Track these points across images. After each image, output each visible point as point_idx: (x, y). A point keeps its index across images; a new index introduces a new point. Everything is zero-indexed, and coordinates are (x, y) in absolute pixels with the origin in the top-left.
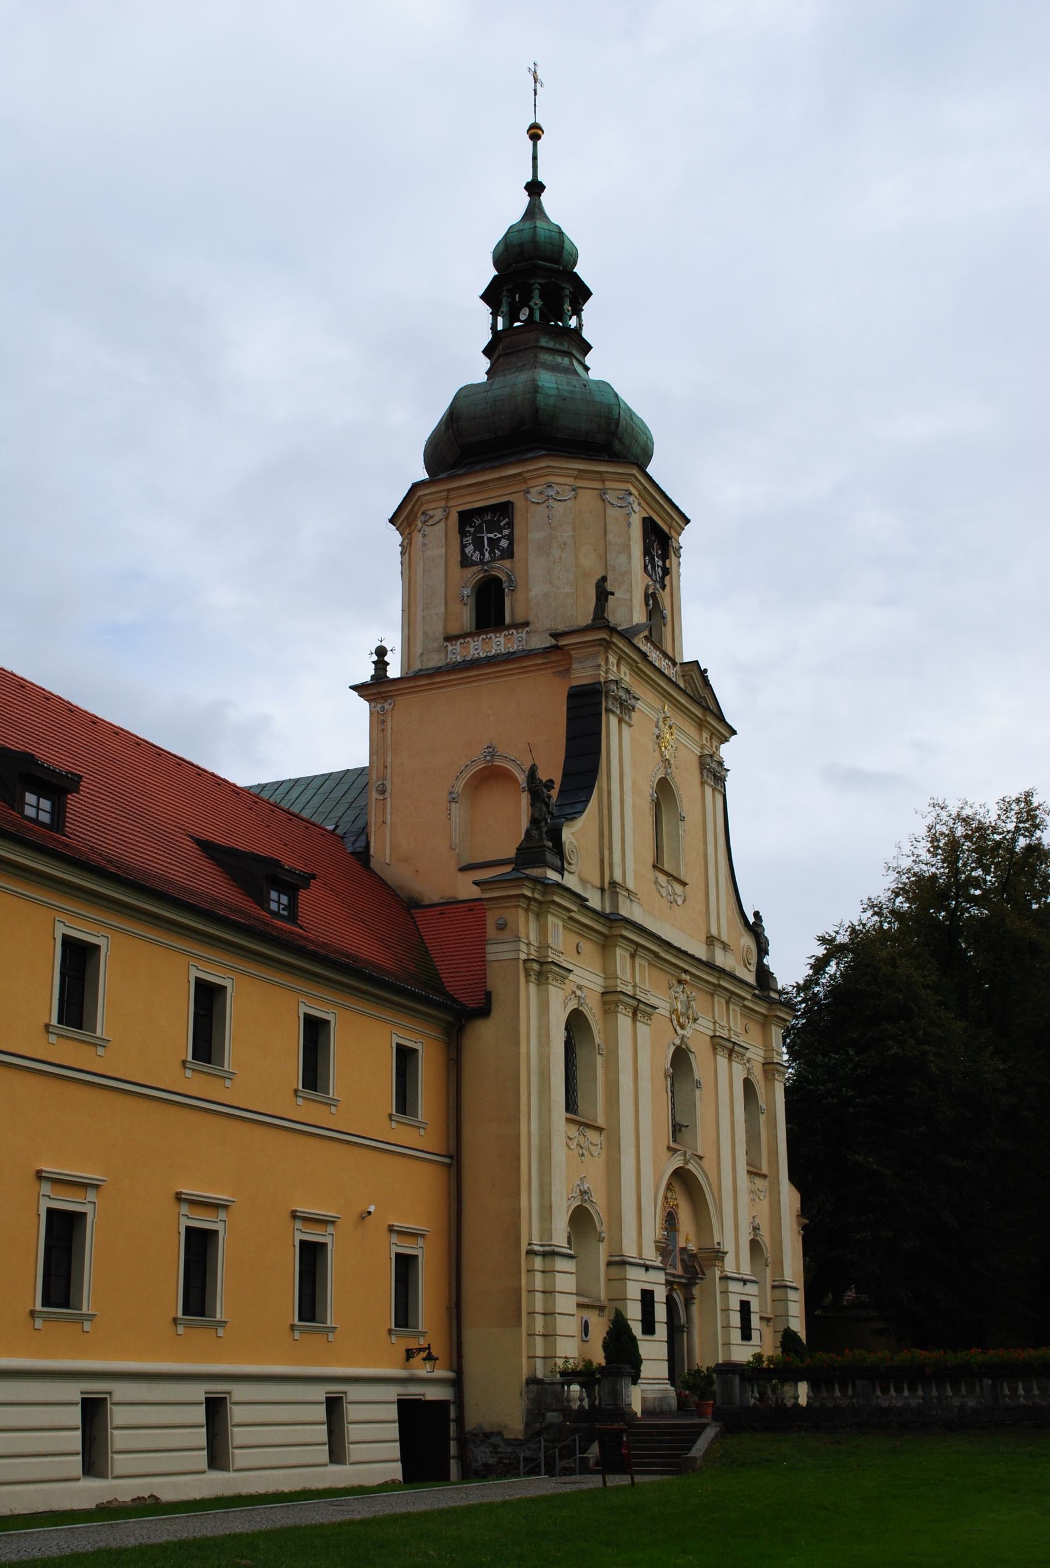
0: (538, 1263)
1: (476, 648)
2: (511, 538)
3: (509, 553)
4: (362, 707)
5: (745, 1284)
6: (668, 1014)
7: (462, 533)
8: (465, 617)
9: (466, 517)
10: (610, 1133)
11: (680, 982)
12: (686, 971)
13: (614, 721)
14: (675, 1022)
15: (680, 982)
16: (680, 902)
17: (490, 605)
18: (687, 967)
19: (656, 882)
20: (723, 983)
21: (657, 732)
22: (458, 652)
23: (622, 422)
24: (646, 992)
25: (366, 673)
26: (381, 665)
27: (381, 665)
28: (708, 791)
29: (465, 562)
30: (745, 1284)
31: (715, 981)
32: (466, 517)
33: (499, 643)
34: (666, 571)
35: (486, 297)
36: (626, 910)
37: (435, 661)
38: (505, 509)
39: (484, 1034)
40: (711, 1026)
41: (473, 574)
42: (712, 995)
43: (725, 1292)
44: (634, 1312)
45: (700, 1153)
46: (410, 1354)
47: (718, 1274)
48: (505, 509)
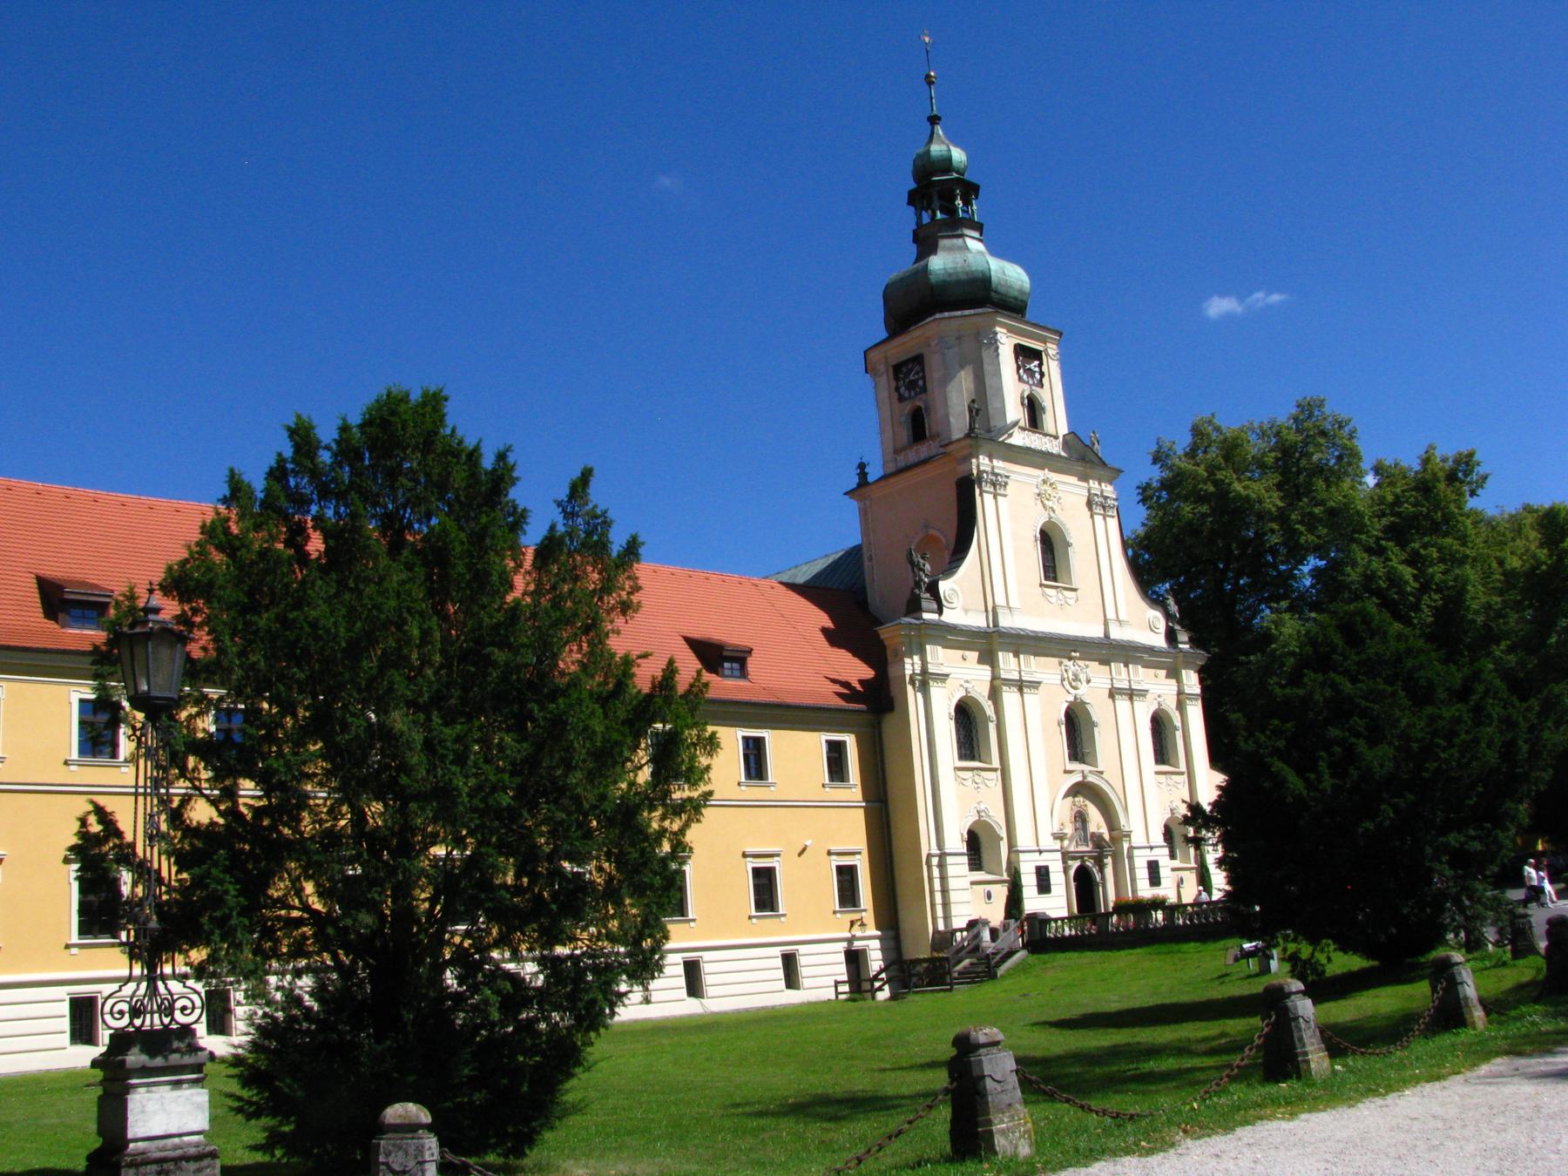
1: (911, 456)
2: (924, 378)
3: (924, 389)
4: (853, 506)
7: (897, 379)
8: (904, 435)
9: (898, 370)
13: (988, 498)
16: (1071, 602)
17: (919, 427)
19: (1044, 594)
22: (902, 461)
23: (994, 279)
24: (1031, 673)
25: (854, 481)
26: (863, 474)
27: (863, 474)
28: (1099, 519)
29: (901, 399)
32: (898, 370)
33: (924, 450)
34: (1042, 375)
35: (909, 203)
36: (1006, 622)
37: (891, 468)
38: (918, 360)
39: (889, 723)
41: (907, 407)
43: (1131, 857)
46: (852, 923)
47: (1126, 846)
48: (918, 360)
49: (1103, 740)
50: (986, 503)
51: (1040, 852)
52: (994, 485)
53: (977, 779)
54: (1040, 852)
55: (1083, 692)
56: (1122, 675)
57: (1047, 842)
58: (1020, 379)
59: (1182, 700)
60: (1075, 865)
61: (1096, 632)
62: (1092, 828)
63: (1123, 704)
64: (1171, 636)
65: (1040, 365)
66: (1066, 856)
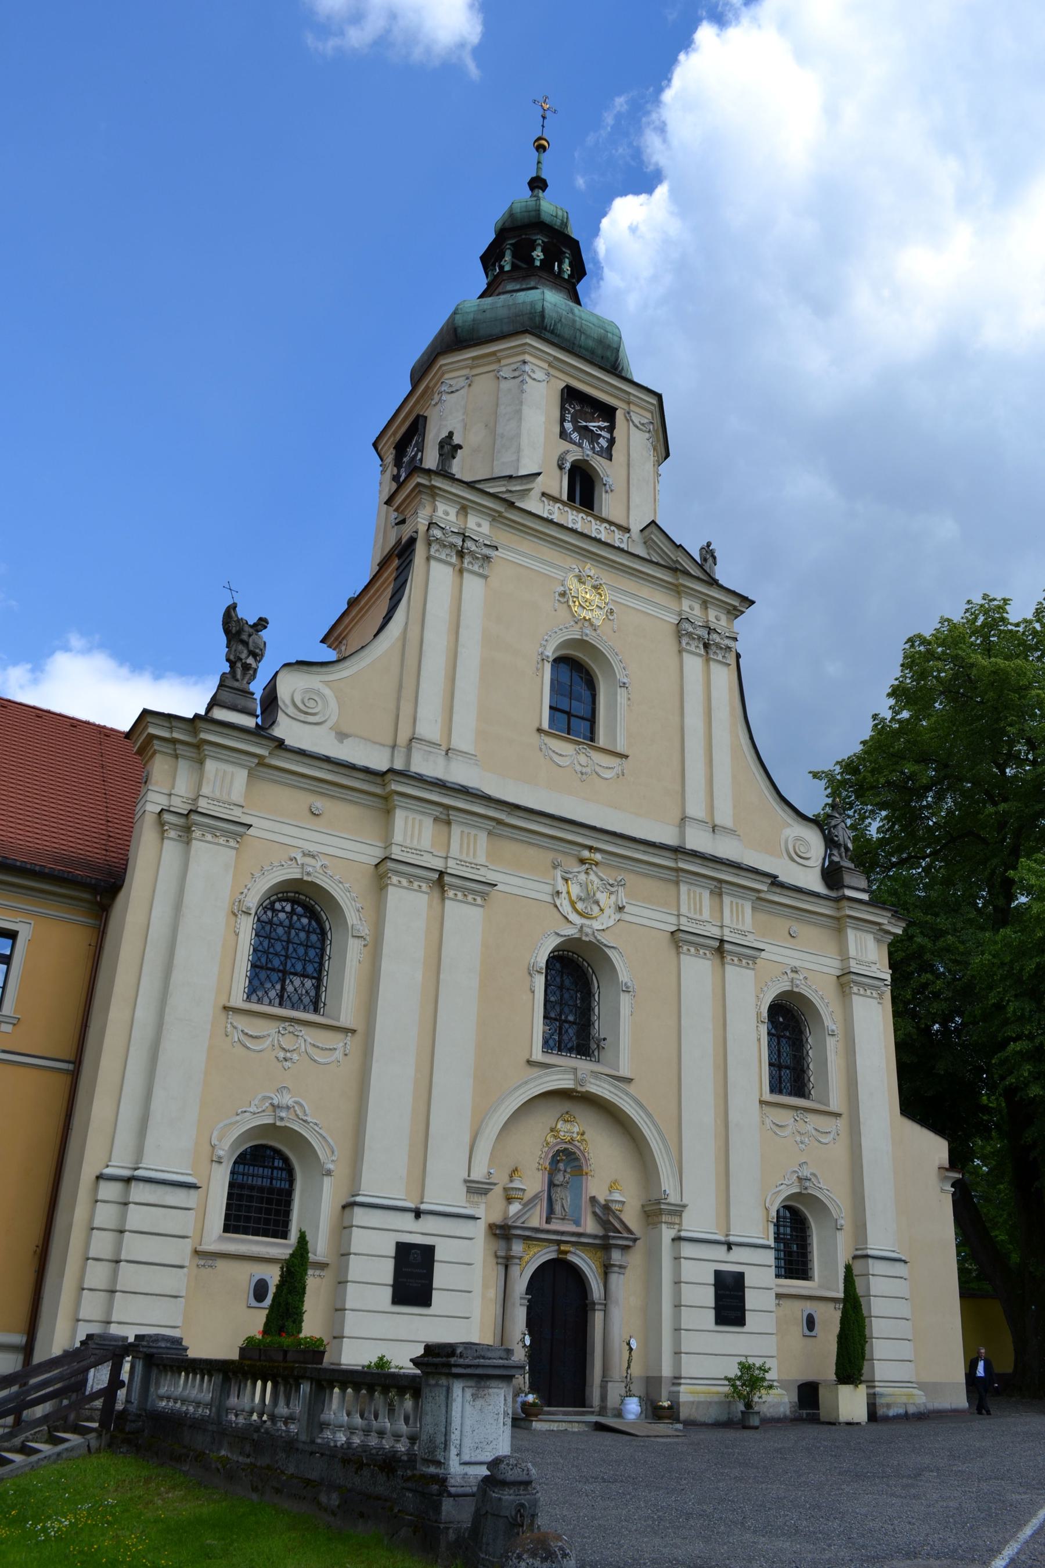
0: (109, 1191)
5: (729, 1248)
6: (549, 899)
10: (363, 1036)
11: (582, 861)
12: (591, 848)
14: (566, 908)
15: (582, 861)
18: (595, 844)
20: (682, 865)
21: (561, 589)
24: (476, 866)
30: (729, 1248)
31: (672, 864)
34: (612, 442)
40: (673, 920)
42: (677, 883)
43: (677, 1258)
44: (373, 1270)
45: (624, 1071)
49: (627, 1019)
50: (434, 579)
51: (418, 1214)
52: (461, 554)
53: (287, 1042)
54: (418, 1214)
55: (601, 925)
56: (697, 908)
57: (445, 1191)
58: (563, 434)
59: (846, 981)
60: (532, 1259)
61: (669, 838)
62: (597, 1187)
63: (698, 969)
64: (832, 875)
65: (611, 429)
66: (502, 1233)
